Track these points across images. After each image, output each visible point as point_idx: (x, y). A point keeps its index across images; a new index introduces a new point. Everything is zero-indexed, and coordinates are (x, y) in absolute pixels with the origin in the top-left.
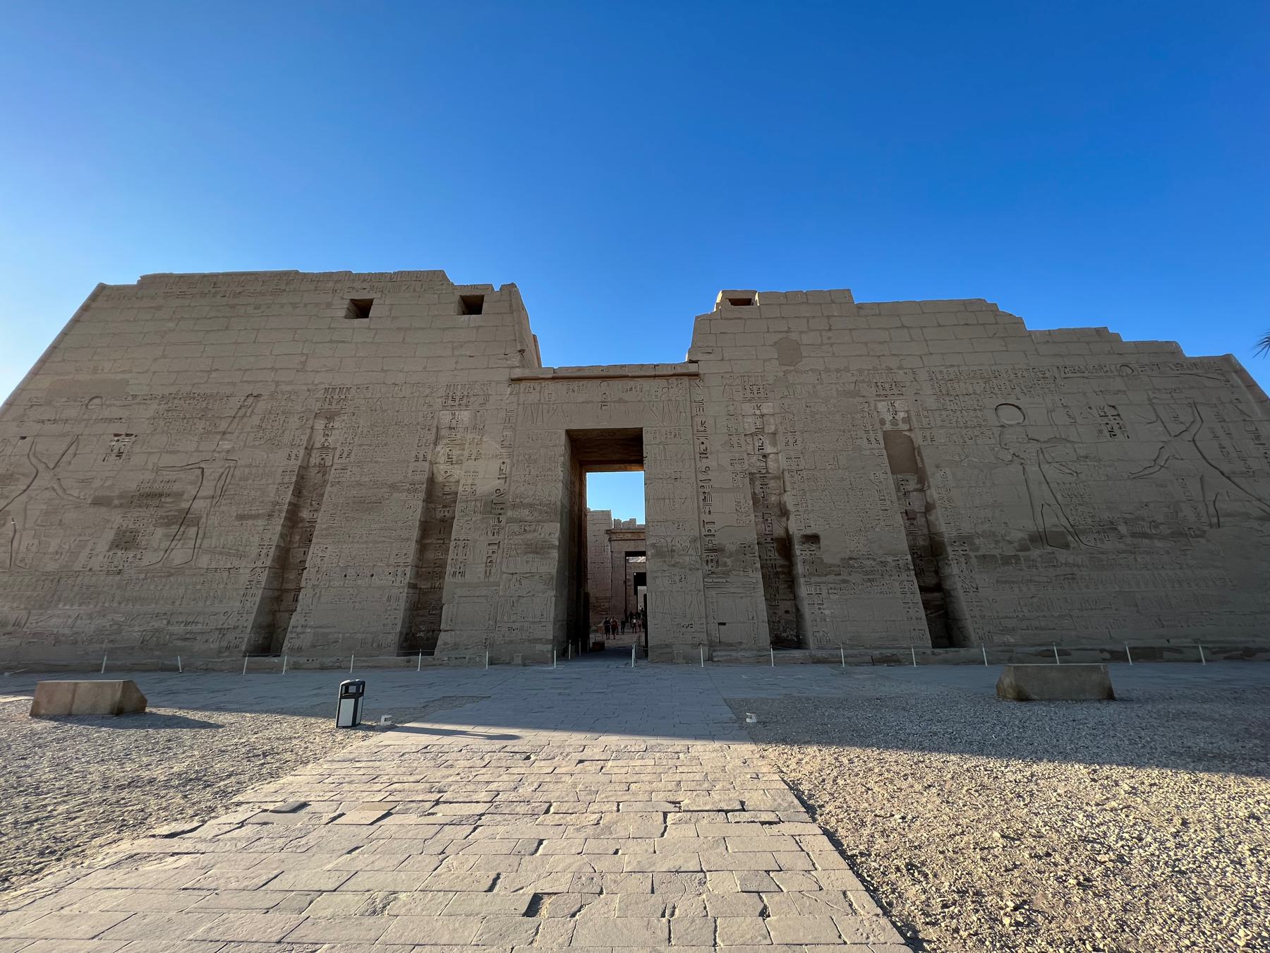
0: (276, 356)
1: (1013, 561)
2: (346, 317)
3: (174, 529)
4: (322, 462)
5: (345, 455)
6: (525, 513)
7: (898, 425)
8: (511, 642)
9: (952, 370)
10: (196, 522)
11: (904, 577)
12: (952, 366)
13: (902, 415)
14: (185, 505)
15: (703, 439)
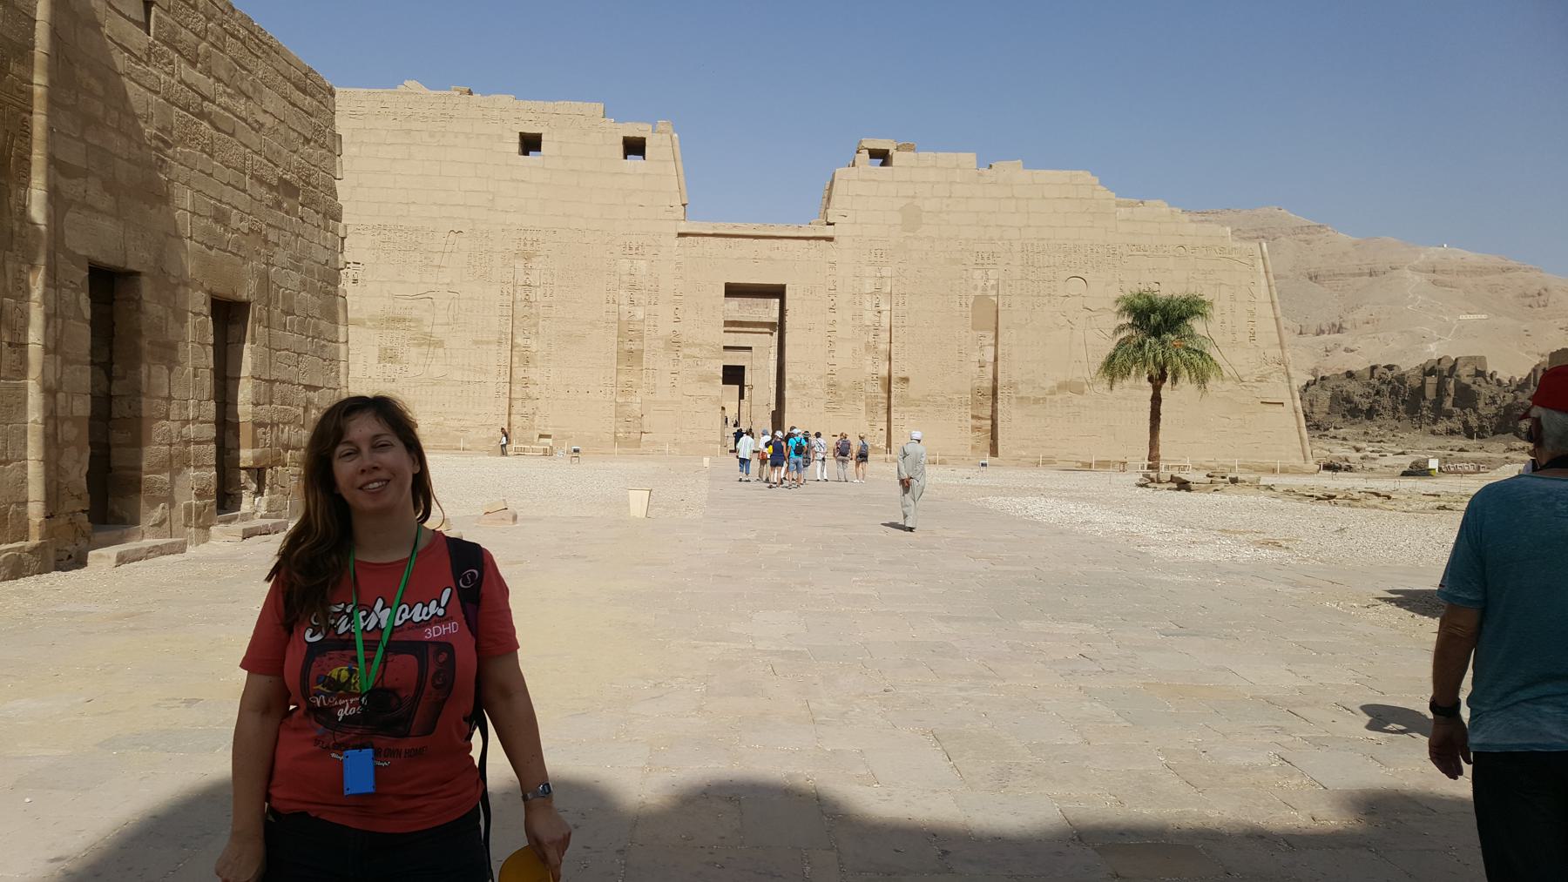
0: (465, 191)
1: (1041, 401)
2: (520, 154)
3: (425, 349)
4: (527, 298)
5: (548, 295)
6: (695, 351)
7: (986, 290)
8: (692, 442)
9: (1041, 243)
10: (440, 344)
11: (963, 410)
12: (1043, 239)
13: (992, 282)
14: (428, 330)
15: (833, 297)
